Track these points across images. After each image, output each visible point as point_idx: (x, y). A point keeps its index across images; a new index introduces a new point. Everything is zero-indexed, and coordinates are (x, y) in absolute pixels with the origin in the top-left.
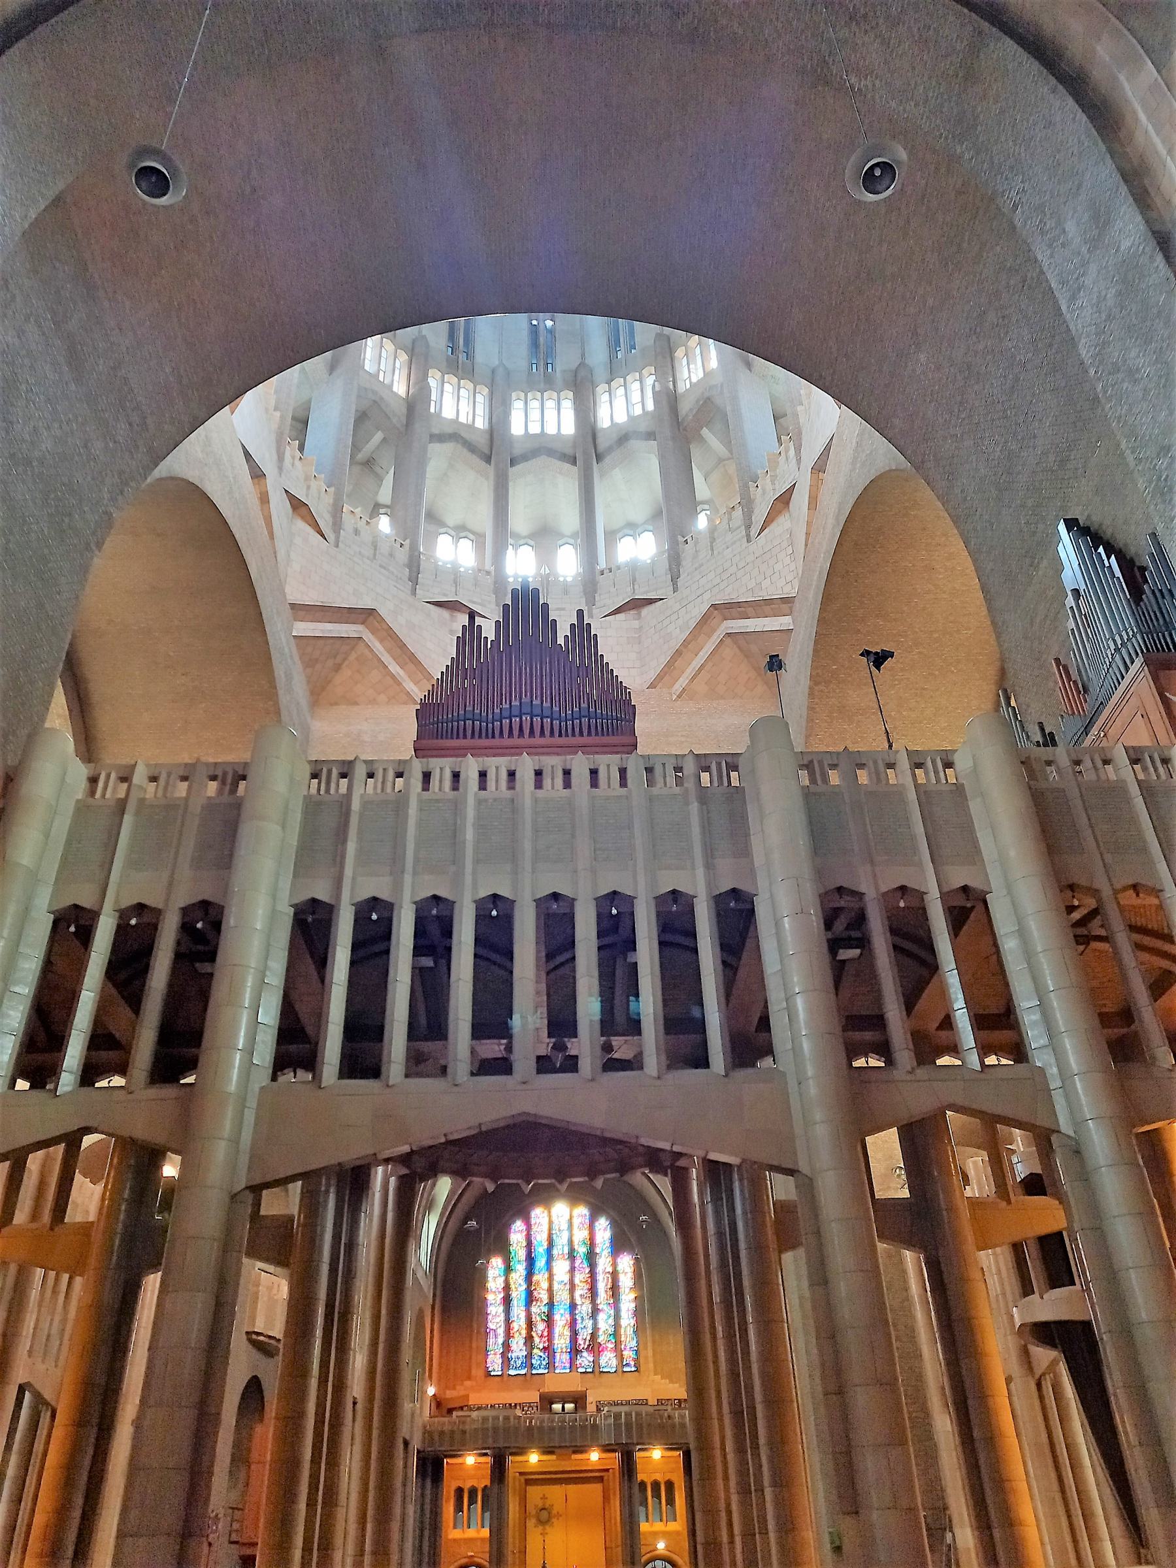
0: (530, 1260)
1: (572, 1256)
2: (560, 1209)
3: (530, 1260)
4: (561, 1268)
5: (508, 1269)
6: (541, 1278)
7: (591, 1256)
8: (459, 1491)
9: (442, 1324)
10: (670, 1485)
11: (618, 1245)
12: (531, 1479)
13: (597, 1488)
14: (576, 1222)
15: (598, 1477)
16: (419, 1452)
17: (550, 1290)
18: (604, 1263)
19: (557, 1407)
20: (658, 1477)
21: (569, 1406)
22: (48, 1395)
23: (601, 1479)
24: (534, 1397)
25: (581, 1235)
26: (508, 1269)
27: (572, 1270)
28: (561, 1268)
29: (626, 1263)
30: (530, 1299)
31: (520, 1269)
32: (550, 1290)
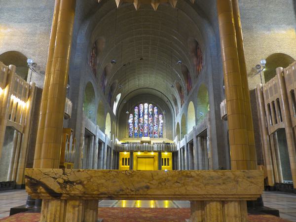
0: (139, 115)
1: (148, 114)
2: (146, 105)
3: (139, 115)
4: (146, 117)
5: (134, 117)
6: (142, 119)
7: (153, 114)
8: (123, 159)
9: (119, 128)
10: (168, 159)
11: (159, 113)
12: (138, 157)
13: (152, 159)
14: (150, 107)
15: (153, 157)
16: (113, 150)
17: (143, 121)
18: (156, 116)
19: (144, 144)
20: (166, 157)
21: (147, 144)
22: (19, 130)
23: (153, 158)
24: (140, 141)
25: (150, 110)
26: (134, 117)
27: (149, 117)
28: (146, 117)
29: (161, 116)
30: (139, 122)
31: (136, 118)
32: (143, 121)
